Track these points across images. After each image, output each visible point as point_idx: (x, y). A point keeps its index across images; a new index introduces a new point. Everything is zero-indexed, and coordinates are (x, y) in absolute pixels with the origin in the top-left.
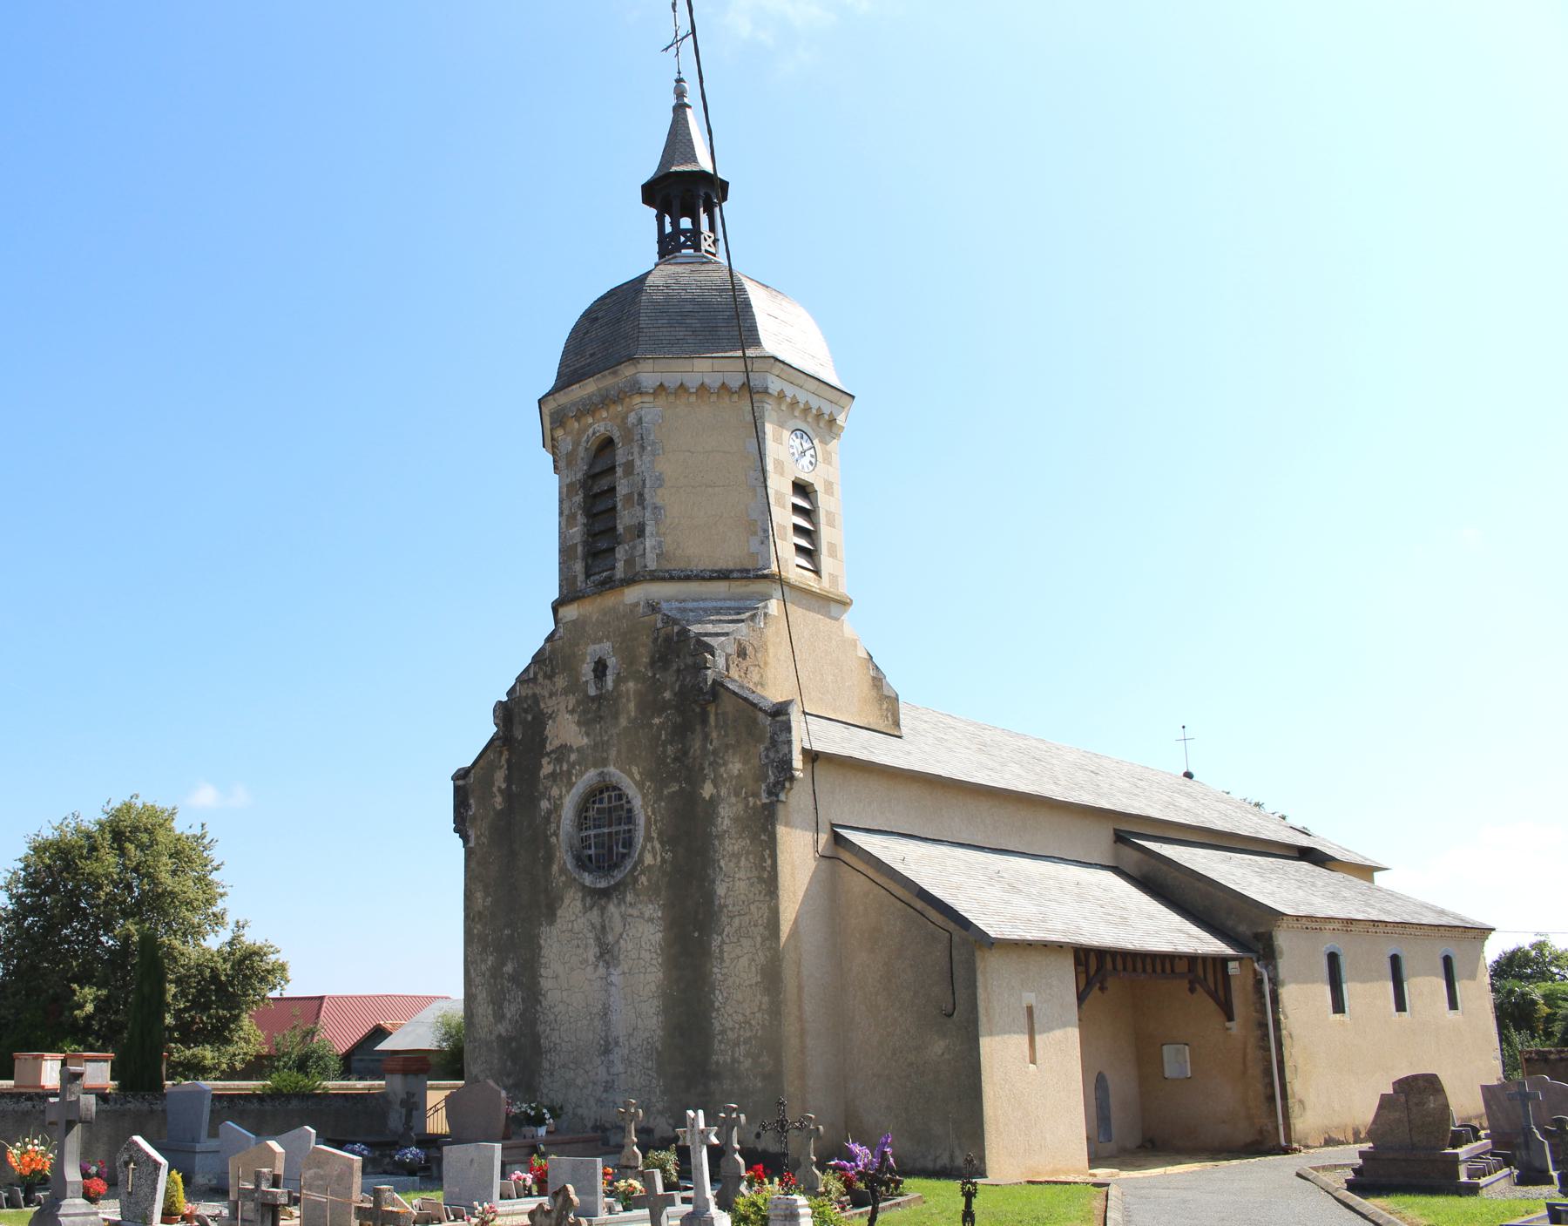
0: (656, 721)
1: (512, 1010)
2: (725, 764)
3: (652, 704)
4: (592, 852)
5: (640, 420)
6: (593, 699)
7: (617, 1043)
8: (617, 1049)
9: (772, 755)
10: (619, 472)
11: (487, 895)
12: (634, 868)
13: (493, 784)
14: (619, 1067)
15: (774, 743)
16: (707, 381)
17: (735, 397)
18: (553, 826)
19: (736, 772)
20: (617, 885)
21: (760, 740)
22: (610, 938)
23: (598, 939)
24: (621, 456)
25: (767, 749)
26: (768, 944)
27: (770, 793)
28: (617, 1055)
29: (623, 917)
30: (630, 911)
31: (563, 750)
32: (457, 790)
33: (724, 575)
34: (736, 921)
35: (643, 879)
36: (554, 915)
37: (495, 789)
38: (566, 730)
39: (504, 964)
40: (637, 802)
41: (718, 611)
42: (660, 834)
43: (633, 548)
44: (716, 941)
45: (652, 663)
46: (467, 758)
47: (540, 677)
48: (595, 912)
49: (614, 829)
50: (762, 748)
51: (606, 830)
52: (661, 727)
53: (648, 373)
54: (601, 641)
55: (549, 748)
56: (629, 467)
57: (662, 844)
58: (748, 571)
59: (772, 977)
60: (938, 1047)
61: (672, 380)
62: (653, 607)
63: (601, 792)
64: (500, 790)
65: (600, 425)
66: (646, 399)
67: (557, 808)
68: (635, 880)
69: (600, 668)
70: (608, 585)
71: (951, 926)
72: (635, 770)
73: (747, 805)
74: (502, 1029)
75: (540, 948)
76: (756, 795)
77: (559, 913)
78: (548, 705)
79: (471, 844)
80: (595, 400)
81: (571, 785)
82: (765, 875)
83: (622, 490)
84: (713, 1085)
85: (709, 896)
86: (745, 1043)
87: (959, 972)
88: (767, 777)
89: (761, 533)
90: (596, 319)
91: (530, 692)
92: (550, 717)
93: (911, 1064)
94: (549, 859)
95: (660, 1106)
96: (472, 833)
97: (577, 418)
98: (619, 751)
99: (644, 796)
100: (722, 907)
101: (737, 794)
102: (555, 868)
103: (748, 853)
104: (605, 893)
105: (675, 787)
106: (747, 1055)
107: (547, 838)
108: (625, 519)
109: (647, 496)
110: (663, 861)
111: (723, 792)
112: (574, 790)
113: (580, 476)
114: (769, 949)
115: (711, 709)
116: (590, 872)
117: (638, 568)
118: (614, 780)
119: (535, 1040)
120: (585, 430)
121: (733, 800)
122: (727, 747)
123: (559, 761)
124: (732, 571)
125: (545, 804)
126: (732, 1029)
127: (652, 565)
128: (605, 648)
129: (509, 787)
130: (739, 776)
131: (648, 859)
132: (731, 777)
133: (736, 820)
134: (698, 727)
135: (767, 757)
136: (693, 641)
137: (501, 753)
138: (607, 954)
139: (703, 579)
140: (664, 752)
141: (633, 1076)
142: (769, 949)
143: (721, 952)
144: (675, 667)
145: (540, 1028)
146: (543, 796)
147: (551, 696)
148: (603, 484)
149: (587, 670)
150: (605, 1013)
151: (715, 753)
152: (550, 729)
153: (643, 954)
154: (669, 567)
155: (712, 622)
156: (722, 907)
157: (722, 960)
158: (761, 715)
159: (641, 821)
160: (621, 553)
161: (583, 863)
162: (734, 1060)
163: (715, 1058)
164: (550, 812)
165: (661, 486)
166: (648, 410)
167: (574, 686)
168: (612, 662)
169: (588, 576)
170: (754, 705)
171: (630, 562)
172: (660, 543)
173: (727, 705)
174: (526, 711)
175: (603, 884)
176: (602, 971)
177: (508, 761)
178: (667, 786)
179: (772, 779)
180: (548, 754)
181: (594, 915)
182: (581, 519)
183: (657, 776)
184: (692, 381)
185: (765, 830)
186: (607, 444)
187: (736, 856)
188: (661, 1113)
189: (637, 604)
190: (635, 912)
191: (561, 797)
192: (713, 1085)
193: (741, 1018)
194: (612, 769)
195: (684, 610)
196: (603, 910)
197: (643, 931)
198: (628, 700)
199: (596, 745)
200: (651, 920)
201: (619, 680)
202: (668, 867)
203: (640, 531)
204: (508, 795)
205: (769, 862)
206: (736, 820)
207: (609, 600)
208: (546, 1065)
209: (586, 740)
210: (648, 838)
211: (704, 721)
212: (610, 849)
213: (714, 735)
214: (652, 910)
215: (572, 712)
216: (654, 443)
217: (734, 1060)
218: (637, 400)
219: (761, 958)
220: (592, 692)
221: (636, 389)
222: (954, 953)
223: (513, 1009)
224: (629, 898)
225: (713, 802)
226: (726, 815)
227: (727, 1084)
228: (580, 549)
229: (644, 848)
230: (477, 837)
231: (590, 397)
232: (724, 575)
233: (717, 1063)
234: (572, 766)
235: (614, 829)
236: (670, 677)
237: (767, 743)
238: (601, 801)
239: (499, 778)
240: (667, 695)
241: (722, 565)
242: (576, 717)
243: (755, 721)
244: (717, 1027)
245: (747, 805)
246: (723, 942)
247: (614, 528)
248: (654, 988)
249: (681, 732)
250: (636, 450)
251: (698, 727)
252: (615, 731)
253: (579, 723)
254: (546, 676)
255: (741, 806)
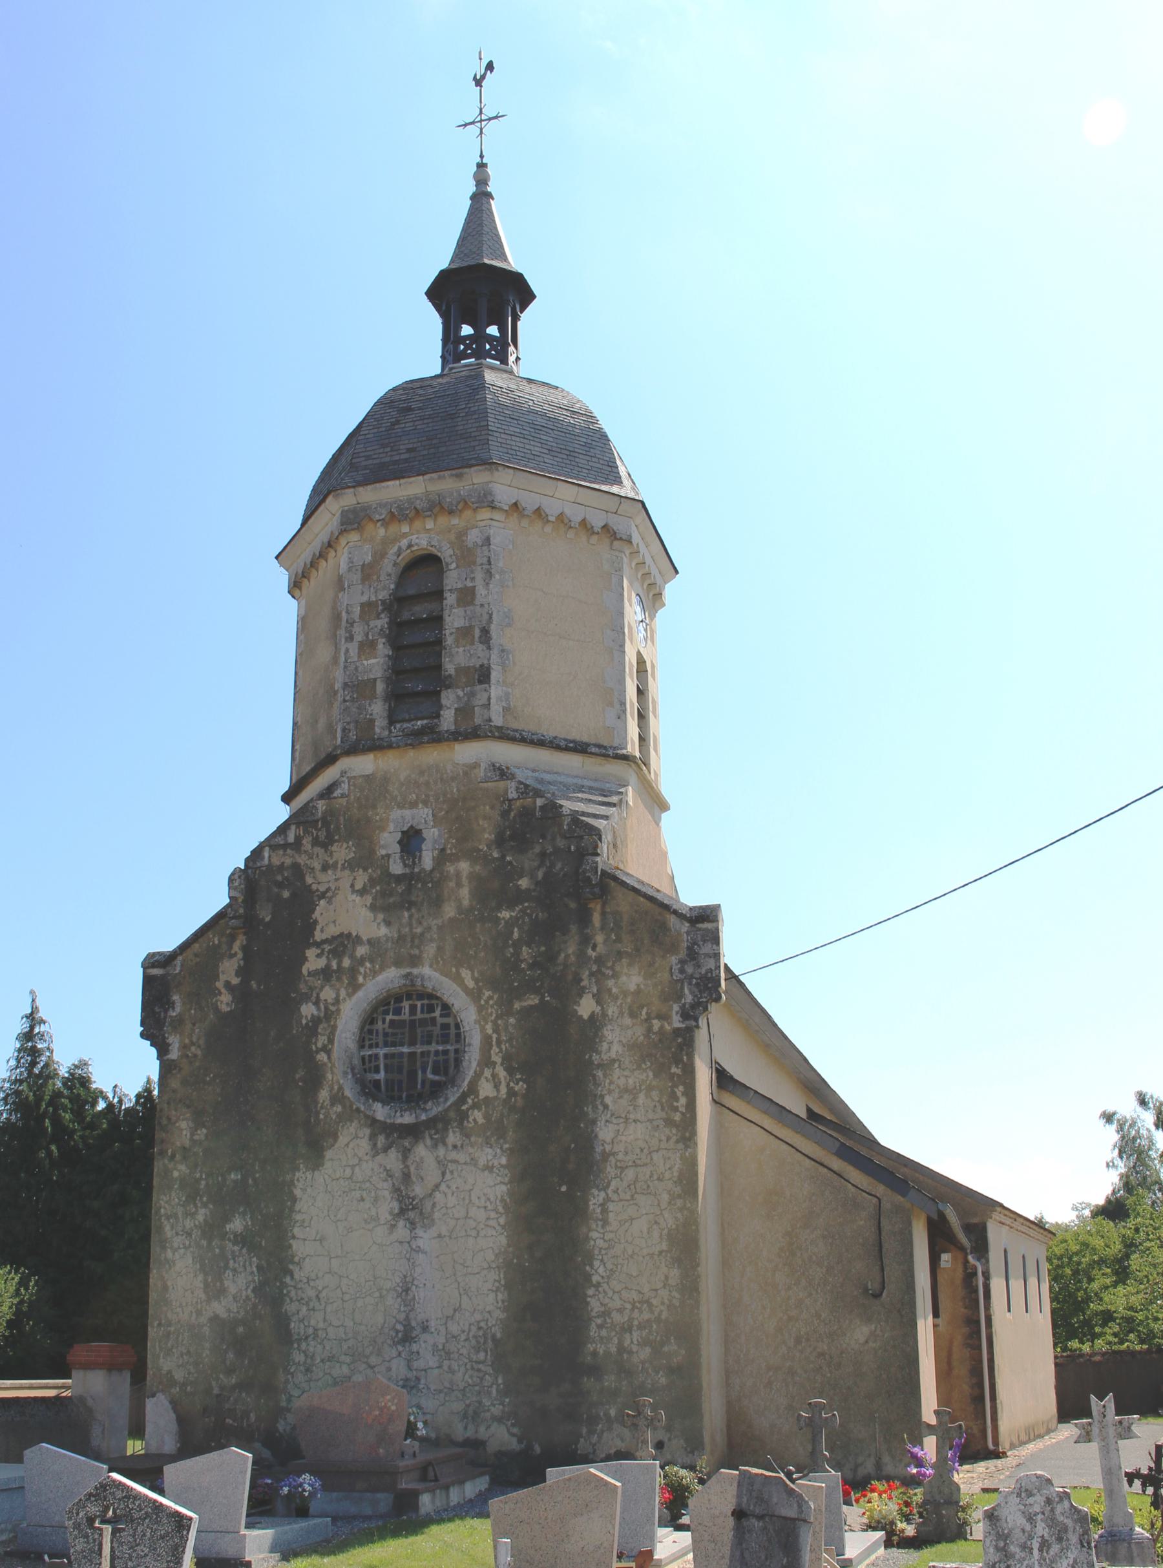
0: (505, 914)
1: (240, 1283)
2: (615, 976)
3: (495, 890)
4: (381, 1076)
5: (487, 541)
6: (399, 879)
7: (425, 1329)
8: (424, 1337)
9: (689, 969)
10: (450, 599)
11: (198, 1124)
12: (463, 1099)
13: (216, 977)
14: (428, 1360)
15: (692, 955)
16: (567, 511)
17: (595, 538)
18: (322, 1040)
19: (632, 987)
20: (432, 1123)
21: (673, 948)
22: (418, 1190)
23: (396, 1190)
24: (453, 579)
25: (682, 962)
26: (679, 1202)
27: (685, 1015)
28: (424, 1345)
29: (442, 1164)
30: (453, 1155)
31: (342, 943)
32: (148, 981)
33: (580, 748)
34: (630, 1174)
35: (478, 1116)
36: (322, 1157)
37: (219, 985)
38: (347, 911)
39: (227, 1219)
40: (468, 1014)
41: (581, 789)
42: (507, 1058)
43: (472, 694)
44: (596, 1199)
45: (500, 841)
46: (169, 944)
47: (307, 843)
48: (393, 1154)
49: (419, 1049)
50: (674, 960)
51: (405, 1050)
52: (510, 924)
53: (505, 486)
54: (413, 805)
55: (318, 936)
56: (467, 596)
57: (510, 1071)
58: (605, 748)
59: (684, 1246)
60: (860, 1334)
61: (530, 502)
62: (503, 773)
63: (399, 999)
64: (228, 984)
65: (422, 537)
66: (497, 516)
67: (330, 1015)
68: (463, 1116)
69: (411, 840)
70: (431, 735)
71: (880, 1189)
72: (466, 974)
73: (649, 1030)
74: (220, 1308)
75: (294, 1200)
76: (664, 1017)
77: (329, 1154)
78: (319, 881)
79: (174, 1055)
80: (419, 505)
81: (354, 987)
82: (677, 1117)
83: (454, 619)
84: (588, 1383)
85: (586, 1142)
86: (640, 1327)
87: (890, 1245)
88: (679, 996)
89: (617, 706)
90: (409, 409)
91: (288, 861)
92: (323, 896)
93: (821, 1355)
94: (315, 1078)
95: (497, 1410)
96: (174, 1041)
97: (385, 523)
98: (440, 949)
99: (480, 1009)
100: (605, 1156)
101: (633, 1015)
102: (324, 1095)
103: (650, 1089)
104: (413, 1132)
105: (533, 1000)
106: (644, 1343)
107: (310, 1057)
108: (456, 658)
109: (494, 633)
110: (511, 1093)
111: (612, 1010)
112: (360, 994)
113: (383, 595)
114: (681, 1210)
115: (596, 908)
116: (384, 1103)
117: (478, 721)
118: (429, 986)
119: (282, 1323)
120: (395, 540)
121: (628, 1021)
122: (620, 955)
123: (337, 953)
124: (588, 745)
125: (308, 1010)
126: (620, 1311)
127: (498, 721)
128: (421, 816)
129: (245, 982)
130: (638, 992)
131: (486, 1089)
132: (625, 994)
133: (632, 1046)
134: (574, 928)
135: (682, 971)
136: (567, 820)
137: (233, 938)
138: (410, 1209)
139: (558, 748)
140: (517, 954)
141: (451, 1371)
142: (681, 1210)
143: (605, 1211)
144: (537, 849)
145: (290, 1307)
146: (306, 998)
147: (325, 868)
148: (421, 610)
149: (388, 842)
150: (406, 1289)
151: (599, 960)
152: (321, 911)
153: (473, 1212)
154: (515, 726)
155: (581, 800)
156: (605, 1156)
157: (605, 1222)
158: (672, 920)
159: (475, 1040)
160: (449, 699)
161: (370, 1090)
162: (621, 1349)
163: (591, 1347)
164: (316, 1021)
165: (509, 625)
166: (502, 532)
167: (365, 858)
168: (431, 834)
169: (392, 721)
170: (667, 907)
171: (465, 711)
172: (507, 694)
173: (623, 903)
174: (280, 885)
175: (407, 1119)
176: (402, 1231)
177: (244, 948)
178: (519, 998)
179: (689, 998)
180: (318, 945)
181: (392, 1160)
182: (383, 649)
183: (506, 983)
184: (552, 508)
185: (677, 1061)
186: (428, 562)
187: (632, 1092)
188: (499, 1420)
189: (476, 766)
190: (462, 1157)
191: (337, 1001)
192: (588, 1383)
193: (634, 1296)
194: (426, 971)
195: (541, 781)
196: (405, 1153)
197: (474, 1185)
198: (459, 885)
199: (401, 939)
200: (489, 1168)
201: (442, 857)
202: (520, 1102)
203: (483, 675)
204: (241, 993)
205: (683, 1101)
206: (632, 1046)
207: (431, 755)
208: (298, 1357)
209: (383, 931)
210: (486, 1062)
211: (584, 918)
212: (412, 1074)
213: (599, 938)
214: (493, 1155)
215: (362, 892)
216: (502, 572)
217: (621, 1349)
218: (485, 514)
219: (669, 1220)
220: (397, 868)
221: (486, 501)
222: (884, 1223)
223: (242, 1280)
224: (453, 1138)
225: (595, 1024)
226: (616, 1040)
227: (610, 1381)
228: (380, 687)
229: (478, 1075)
230: (184, 1047)
231: (410, 500)
232: (580, 748)
233: (595, 1354)
234: (361, 962)
235: (419, 1049)
236: (528, 861)
237: (683, 954)
238: (398, 1011)
239: (229, 971)
240: (524, 883)
241: (576, 734)
242: (369, 899)
243: (664, 926)
244: (595, 1305)
245: (649, 1030)
246: (608, 1199)
247: (439, 667)
248: (490, 1256)
249: (545, 932)
250: (479, 575)
251: (574, 928)
252: (434, 923)
253: (373, 908)
254: (316, 842)
255: (639, 1032)
